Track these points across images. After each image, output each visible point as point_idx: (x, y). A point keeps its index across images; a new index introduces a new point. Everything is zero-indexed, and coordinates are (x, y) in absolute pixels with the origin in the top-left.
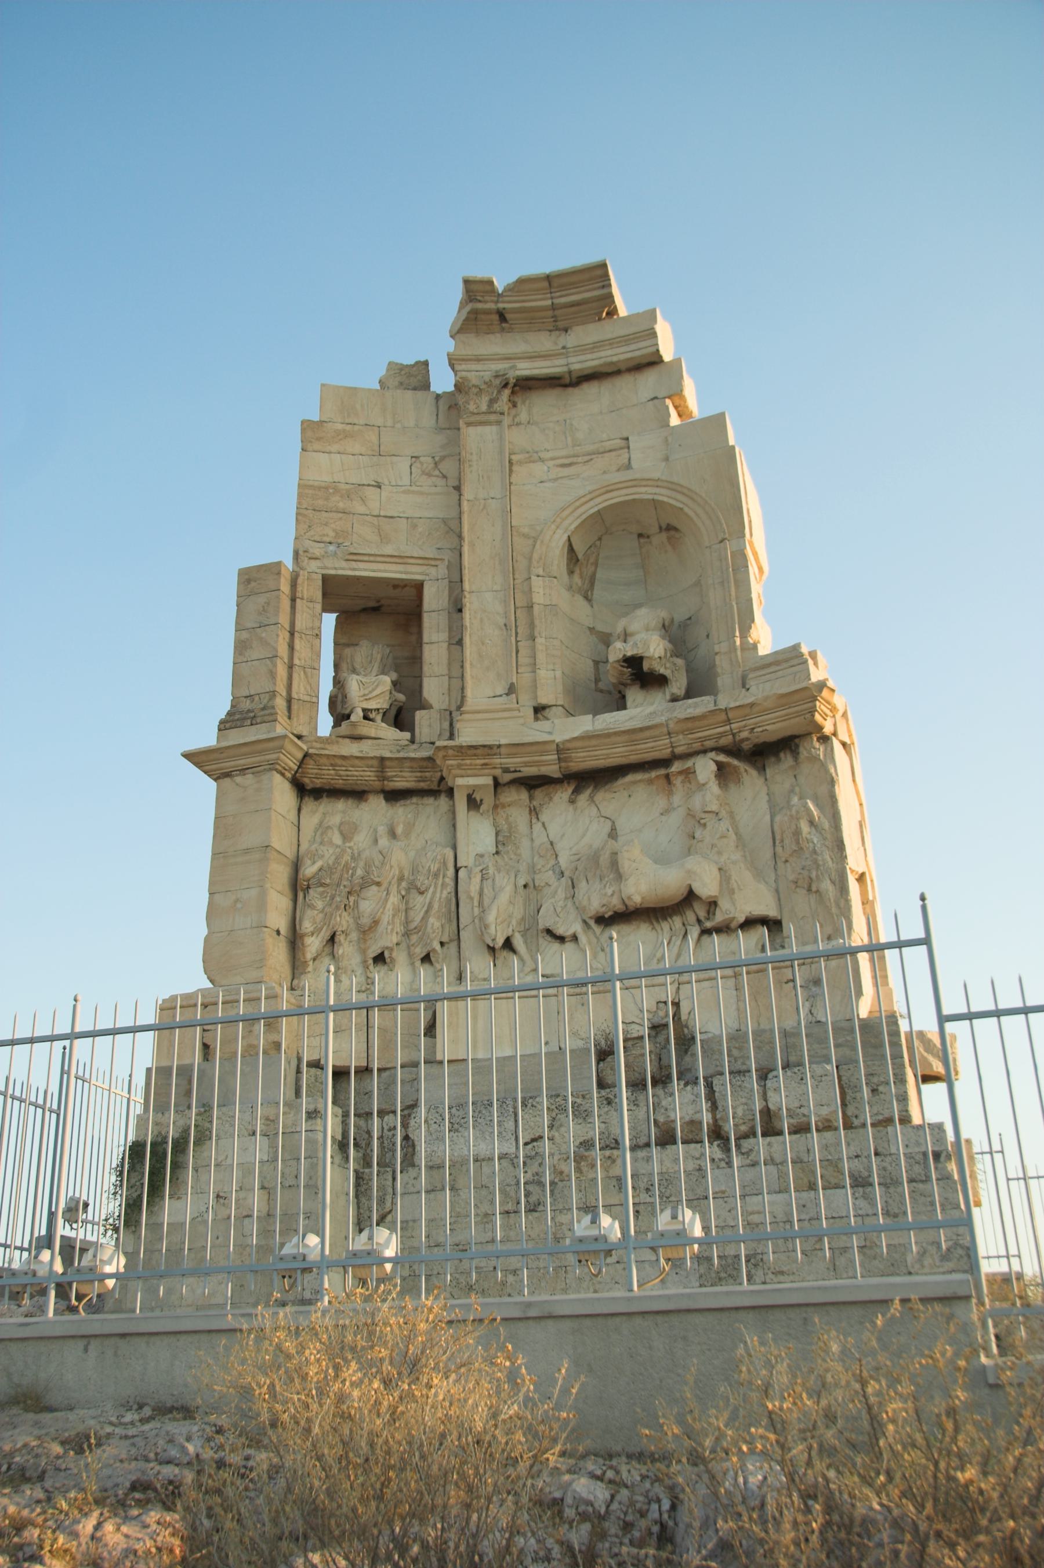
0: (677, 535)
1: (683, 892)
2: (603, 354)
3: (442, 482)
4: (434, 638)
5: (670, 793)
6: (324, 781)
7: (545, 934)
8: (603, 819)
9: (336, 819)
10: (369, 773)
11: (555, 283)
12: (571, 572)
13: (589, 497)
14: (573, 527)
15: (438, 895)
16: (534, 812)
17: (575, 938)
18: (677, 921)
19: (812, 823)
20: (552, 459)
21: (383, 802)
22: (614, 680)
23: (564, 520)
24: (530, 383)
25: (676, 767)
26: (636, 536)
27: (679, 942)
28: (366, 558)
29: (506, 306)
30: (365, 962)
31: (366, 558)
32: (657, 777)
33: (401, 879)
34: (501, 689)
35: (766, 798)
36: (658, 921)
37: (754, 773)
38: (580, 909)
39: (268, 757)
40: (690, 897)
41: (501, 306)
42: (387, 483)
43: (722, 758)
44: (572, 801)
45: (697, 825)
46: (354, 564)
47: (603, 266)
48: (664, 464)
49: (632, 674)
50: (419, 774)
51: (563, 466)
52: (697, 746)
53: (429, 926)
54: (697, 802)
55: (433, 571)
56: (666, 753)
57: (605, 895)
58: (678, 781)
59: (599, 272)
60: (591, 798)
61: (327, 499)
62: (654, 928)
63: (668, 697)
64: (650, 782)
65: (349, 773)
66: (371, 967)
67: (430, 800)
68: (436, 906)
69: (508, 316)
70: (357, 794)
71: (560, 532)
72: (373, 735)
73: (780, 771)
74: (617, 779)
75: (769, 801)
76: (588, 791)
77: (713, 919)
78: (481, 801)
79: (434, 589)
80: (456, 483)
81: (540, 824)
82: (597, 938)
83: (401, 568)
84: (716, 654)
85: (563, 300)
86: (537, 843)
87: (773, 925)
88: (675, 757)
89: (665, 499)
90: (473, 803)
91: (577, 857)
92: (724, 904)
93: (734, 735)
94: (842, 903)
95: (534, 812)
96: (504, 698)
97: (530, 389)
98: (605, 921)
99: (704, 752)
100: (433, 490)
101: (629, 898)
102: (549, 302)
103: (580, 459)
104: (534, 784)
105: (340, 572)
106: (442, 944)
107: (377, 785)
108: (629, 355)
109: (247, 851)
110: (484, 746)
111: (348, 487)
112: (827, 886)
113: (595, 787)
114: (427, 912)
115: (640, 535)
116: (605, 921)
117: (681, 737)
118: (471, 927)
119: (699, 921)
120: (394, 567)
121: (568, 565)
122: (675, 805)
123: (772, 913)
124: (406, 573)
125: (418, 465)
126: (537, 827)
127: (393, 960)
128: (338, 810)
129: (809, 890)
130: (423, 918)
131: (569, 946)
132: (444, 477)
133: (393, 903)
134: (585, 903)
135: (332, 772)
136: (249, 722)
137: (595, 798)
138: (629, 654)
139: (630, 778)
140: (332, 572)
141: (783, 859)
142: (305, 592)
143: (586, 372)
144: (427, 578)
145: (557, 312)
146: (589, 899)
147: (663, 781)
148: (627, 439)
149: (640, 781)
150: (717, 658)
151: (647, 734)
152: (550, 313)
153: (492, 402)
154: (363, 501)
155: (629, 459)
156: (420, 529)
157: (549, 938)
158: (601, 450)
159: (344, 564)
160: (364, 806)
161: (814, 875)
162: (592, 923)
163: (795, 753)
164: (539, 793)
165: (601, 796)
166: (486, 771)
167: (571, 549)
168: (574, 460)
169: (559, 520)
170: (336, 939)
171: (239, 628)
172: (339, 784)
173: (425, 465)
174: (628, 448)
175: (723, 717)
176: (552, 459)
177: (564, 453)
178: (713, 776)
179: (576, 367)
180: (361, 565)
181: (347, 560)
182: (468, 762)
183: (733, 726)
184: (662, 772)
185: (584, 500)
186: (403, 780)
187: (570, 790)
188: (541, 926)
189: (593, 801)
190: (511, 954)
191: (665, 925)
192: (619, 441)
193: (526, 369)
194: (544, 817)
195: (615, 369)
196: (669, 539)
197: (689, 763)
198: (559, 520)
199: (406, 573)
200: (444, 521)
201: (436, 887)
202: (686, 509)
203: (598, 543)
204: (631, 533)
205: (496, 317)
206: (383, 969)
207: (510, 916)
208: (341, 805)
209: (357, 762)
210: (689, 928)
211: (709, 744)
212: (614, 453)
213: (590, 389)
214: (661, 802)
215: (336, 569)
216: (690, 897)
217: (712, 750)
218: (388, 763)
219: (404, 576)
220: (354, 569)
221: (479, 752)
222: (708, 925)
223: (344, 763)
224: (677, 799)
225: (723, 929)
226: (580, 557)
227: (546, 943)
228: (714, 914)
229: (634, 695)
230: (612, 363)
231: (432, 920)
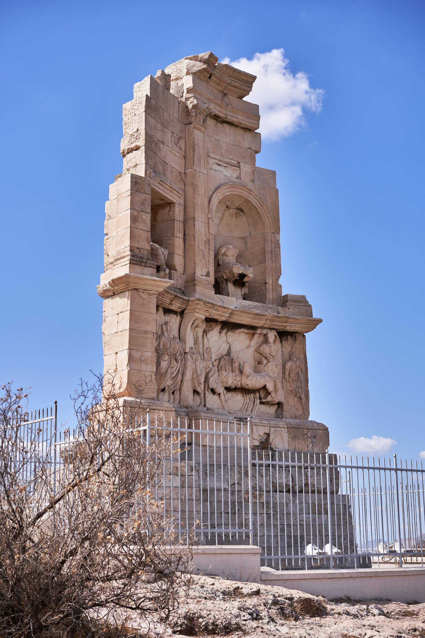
0: (241, 213)
1: (262, 385)
2: (239, 117)
3: (180, 151)
4: (178, 236)
5: (251, 340)
7: (209, 390)
8: (227, 343)
16: (205, 332)
17: (219, 394)
18: (252, 395)
19: (301, 370)
20: (214, 159)
22: (225, 277)
25: (259, 331)
27: (252, 405)
28: (164, 185)
29: (216, 73)
30: (158, 390)
31: (164, 185)
32: (251, 333)
34: (204, 274)
35: (281, 353)
36: (246, 394)
38: (223, 382)
39: (158, 289)
40: (264, 388)
41: (214, 72)
44: (220, 333)
45: (264, 359)
48: (252, 183)
49: (236, 279)
51: (217, 164)
52: (271, 327)
53: (179, 378)
54: (266, 349)
55: (178, 199)
57: (236, 380)
58: (256, 336)
59: (250, 80)
60: (226, 333)
62: (243, 396)
63: (243, 293)
64: (248, 334)
65: (165, 299)
67: (175, 316)
68: (181, 368)
69: (213, 78)
73: (288, 345)
74: (237, 329)
75: (282, 354)
76: (226, 330)
77: (266, 399)
79: (178, 209)
80: (184, 155)
81: (207, 339)
84: (266, 283)
85: (234, 83)
86: (205, 348)
87: (280, 405)
88: (262, 328)
89: (253, 202)
91: (218, 357)
92: (273, 394)
93: (285, 327)
94: (307, 404)
95: (205, 332)
96: (205, 277)
98: (228, 389)
99: (271, 329)
100: (178, 154)
101: (248, 385)
104: (209, 320)
107: (167, 306)
108: (248, 124)
109: (146, 332)
110: (212, 304)
112: (303, 396)
114: (179, 371)
115: (227, 207)
116: (228, 389)
117: (269, 321)
118: (190, 382)
119: (260, 398)
122: (251, 345)
126: (206, 340)
129: (296, 396)
130: (177, 374)
131: (216, 397)
132: (181, 149)
134: (225, 380)
136: (144, 264)
137: (228, 334)
139: (242, 330)
141: (288, 380)
146: (227, 379)
148: (239, 163)
149: (246, 332)
150: (267, 285)
151: (260, 317)
152: (226, 85)
153: (204, 121)
154: (160, 150)
155: (240, 173)
157: (211, 392)
158: (231, 163)
159: (157, 184)
161: (300, 391)
162: (224, 388)
163: (295, 339)
165: (230, 333)
171: (132, 208)
173: (175, 139)
174: (239, 167)
175: (287, 320)
176: (214, 159)
177: (218, 157)
179: (229, 117)
181: (159, 183)
183: (287, 324)
184: (254, 332)
186: (176, 306)
187: (220, 327)
188: (210, 387)
189: (226, 335)
191: (248, 397)
192: (236, 162)
194: (209, 336)
196: (236, 213)
197: (265, 332)
200: (180, 173)
202: (259, 210)
205: (209, 75)
206: (162, 393)
210: (256, 400)
211: (275, 327)
212: (234, 167)
213: (227, 127)
214: (247, 342)
215: (155, 186)
216: (264, 388)
217: (274, 329)
218: (176, 298)
220: (160, 189)
221: (209, 305)
222: (264, 400)
224: (253, 343)
225: (267, 403)
227: (208, 393)
228: (267, 397)
229: (231, 287)
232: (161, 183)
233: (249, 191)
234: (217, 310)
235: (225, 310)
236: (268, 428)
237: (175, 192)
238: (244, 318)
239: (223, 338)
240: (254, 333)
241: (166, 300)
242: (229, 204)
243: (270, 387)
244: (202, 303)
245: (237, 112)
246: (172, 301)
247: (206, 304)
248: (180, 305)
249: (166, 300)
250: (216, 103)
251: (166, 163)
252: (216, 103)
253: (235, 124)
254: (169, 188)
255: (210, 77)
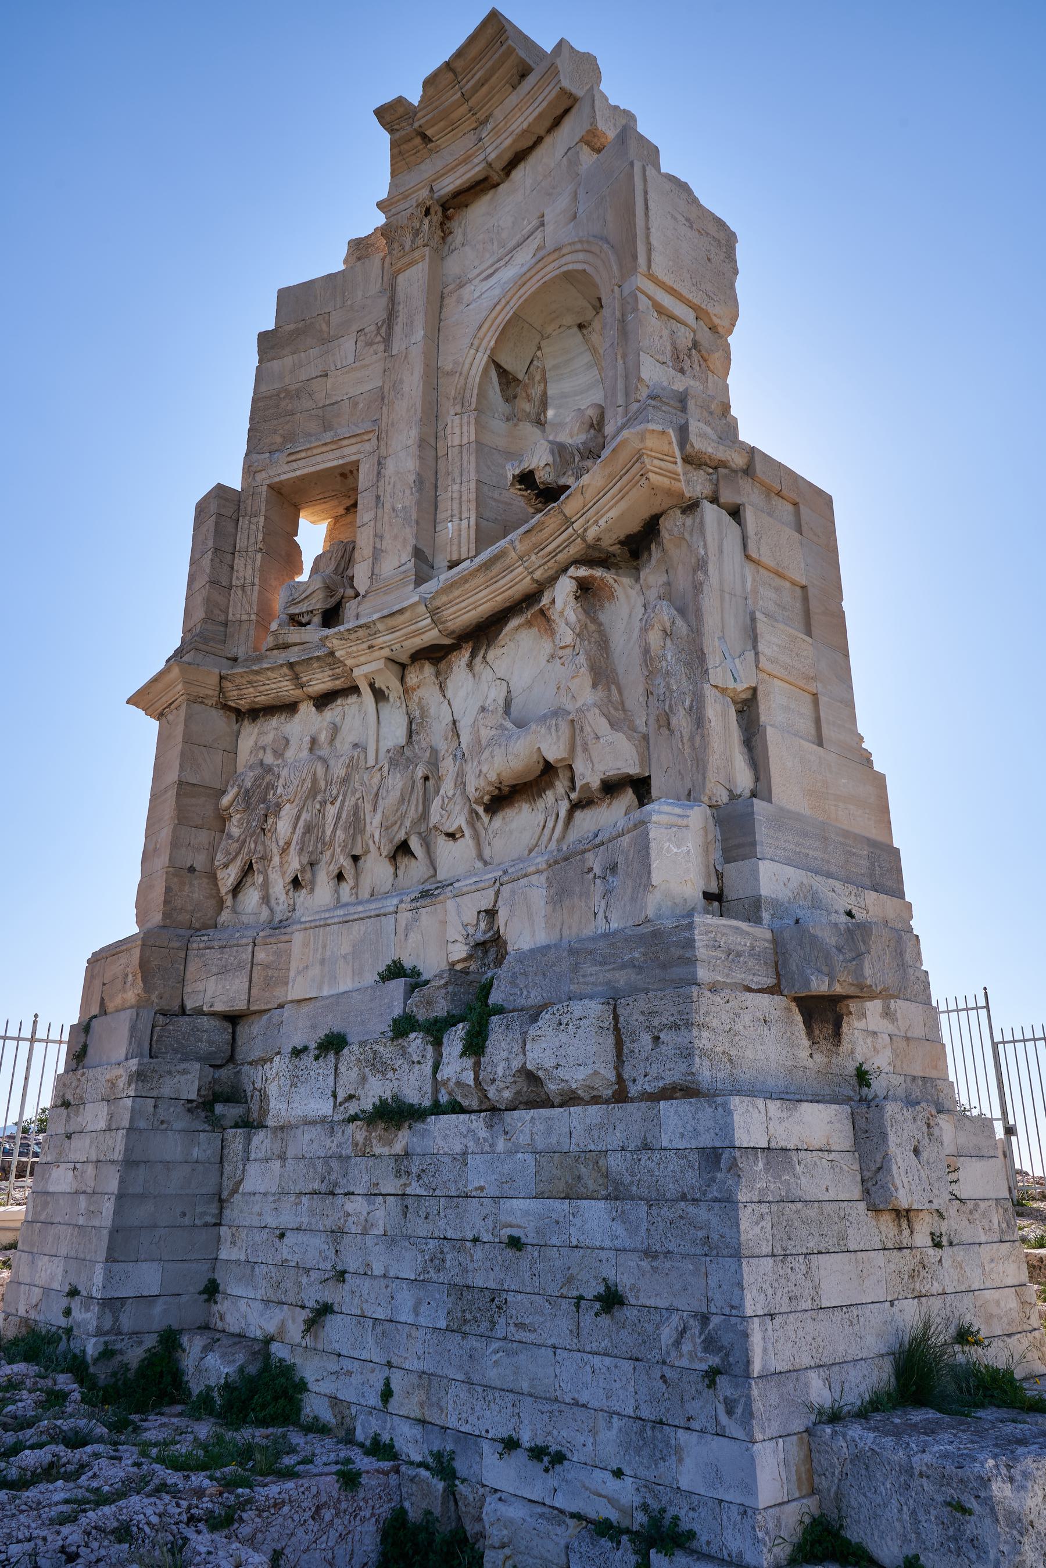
6: (248, 700)
9: (268, 738)
10: (286, 683)
11: (459, 65)
12: (510, 399)
13: (503, 302)
14: (493, 343)
15: (346, 804)
21: (314, 709)
23: (482, 340)
24: (461, 198)
26: (576, 329)
28: (303, 455)
31: (303, 455)
33: (314, 791)
37: (626, 581)
42: (333, 368)
43: (583, 572)
46: (295, 465)
47: (494, 16)
50: (330, 673)
56: (525, 585)
61: (278, 406)
64: (529, 624)
65: (267, 687)
66: (291, 893)
68: (344, 816)
69: (429, 133)
70: (290, 708)
71: (480, 354)
72: (298, 641)
78: (388, 688)
82: (486, 829)
83: (337, 453)
90: (379, 695)
92: (579, 767)
97: (466, 206)
102: (459, 94)
103: (502, 263)
105: (284, 477)
106: (356, 859)
111: (297, 386)
113: (489, 646)
115: (581, 326)
120: (331, 455)
121: (502, 391)
123: (633, 769)
124: (342, 457)
125: (362, 338)
127: (313, 883)
128: (273, 726)
133: (305, 820)
135: (251, 690)
137: (488, 659)
138: (517, 472)
140: (277, 479)
142: (249, 508)
143: (508, 156)
144: (362, 456)
145: (472, 102)
147: (541, 619)
152: (464, 108)
156: (361, 406)
159: (286, 468)
160: (298, 717)
164: (442, 665)
165: (491, 655)
166: (377, 654)
167: (503, 373)
168: (497, 265)
169: (476, 342)
170: (255, 866)
172: (262, 700)
177: (490, 262)
178: (572, 597)
180: (301, 463)
182: (354, 648)
185: (498, 308)
186: (320, 681)
189: (487, 663)
190: (413, 860)
193: (449, 184)
195: (534, 139)
198: (476, 342)
199: (342, 457)
201: (345, 796)
203: (539, 353)
204: (569, 327)
205: (418, 140)
207: (403, 817)
208: (274, 722)
209: (269, 673)
214: (546, 647)
218: (298, 668)
219: (341, 462)
220: (296, 470)
223: (259, 678)
226: (520, 376)
230: (524, 132)
231: (338, 833)
232: (293, 457)
233: (556, 255)
234: (393, 630)
235: (407, 615)
236: (491, 893)
237: (345, 442)
238: (471, 600)
239: (483, 677)
240: (542, 612)
241: (273, 686)
242: (569, 320)
243: (554, 753)
244: (335, 642)
245: (506, 123)
246: (297, 677)
247: (353, 636)
248: (330, 673)
249: (273, 686)
250: (453, 169)
251: (336, 403)
252: (453, 169)
253: (531, 143)
254: (324, 449)
255: (426, 139)
